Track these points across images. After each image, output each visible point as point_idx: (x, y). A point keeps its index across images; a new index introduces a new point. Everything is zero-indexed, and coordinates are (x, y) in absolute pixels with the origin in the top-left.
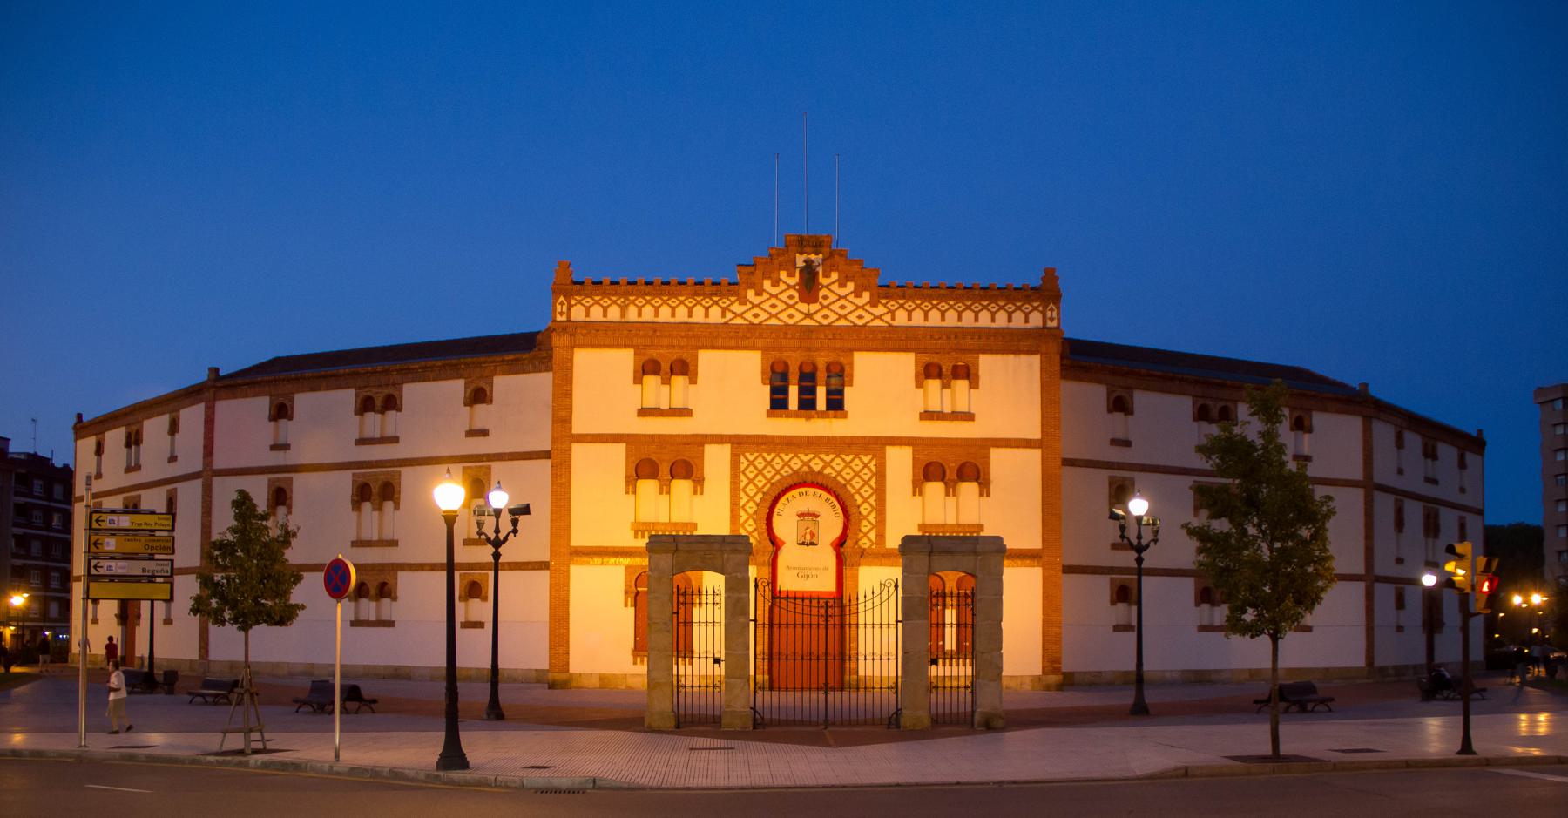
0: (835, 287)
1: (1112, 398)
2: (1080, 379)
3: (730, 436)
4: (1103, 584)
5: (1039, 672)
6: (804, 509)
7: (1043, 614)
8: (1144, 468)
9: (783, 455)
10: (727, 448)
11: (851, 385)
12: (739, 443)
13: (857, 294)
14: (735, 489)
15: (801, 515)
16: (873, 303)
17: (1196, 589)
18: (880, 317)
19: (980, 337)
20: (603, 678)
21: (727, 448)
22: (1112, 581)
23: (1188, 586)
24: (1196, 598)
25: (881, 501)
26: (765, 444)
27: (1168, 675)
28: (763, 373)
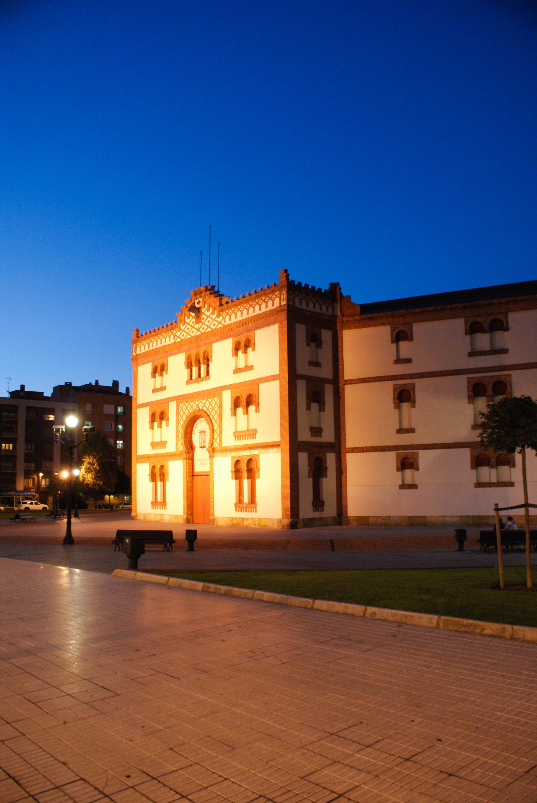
0: (206, 313)
1: (395, 333)
2: (369, 326)
3: (176, 397)
4: (391, 457)
5: (280, 517)
6: (201, 430)
7: (282, 481)
8: (421, 375)
9: (202, 401)
10: (175, 402)
11: (212, 361)
12: (179, 399)
13: (213, 313)
14: (178, 423)
15: (200, 432)
16: (218, 316)
17: (471, 456)
18: (220, 323)
19: (254, 321)
20: (144, 515)
21: (175, 402)
22: (398, 456)
23: (466, 454)
24: (472, 464)
25: (221, 421)
26: (185, 398)
27: (448, 519)
28: (185, 363)
